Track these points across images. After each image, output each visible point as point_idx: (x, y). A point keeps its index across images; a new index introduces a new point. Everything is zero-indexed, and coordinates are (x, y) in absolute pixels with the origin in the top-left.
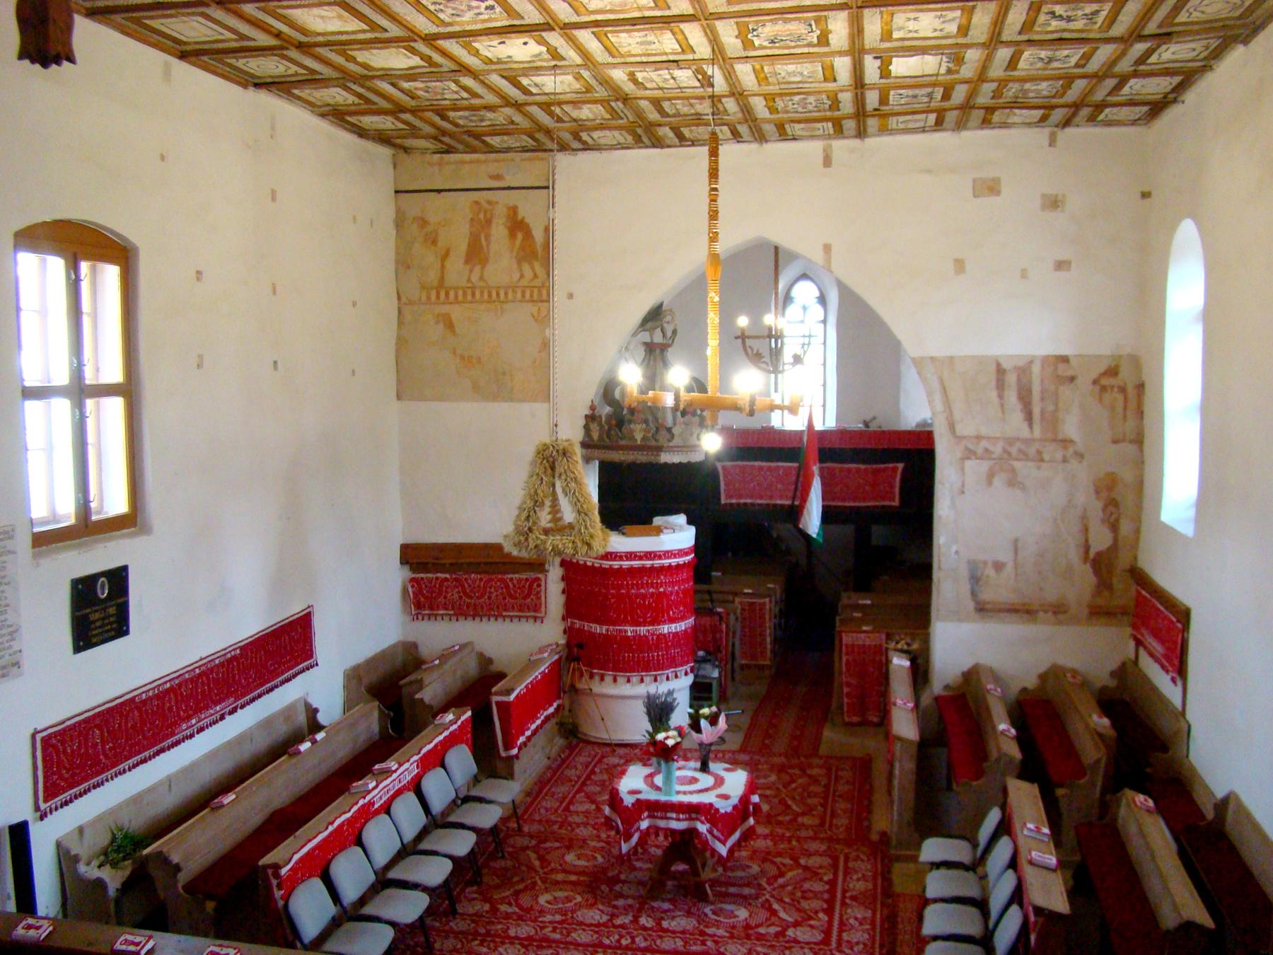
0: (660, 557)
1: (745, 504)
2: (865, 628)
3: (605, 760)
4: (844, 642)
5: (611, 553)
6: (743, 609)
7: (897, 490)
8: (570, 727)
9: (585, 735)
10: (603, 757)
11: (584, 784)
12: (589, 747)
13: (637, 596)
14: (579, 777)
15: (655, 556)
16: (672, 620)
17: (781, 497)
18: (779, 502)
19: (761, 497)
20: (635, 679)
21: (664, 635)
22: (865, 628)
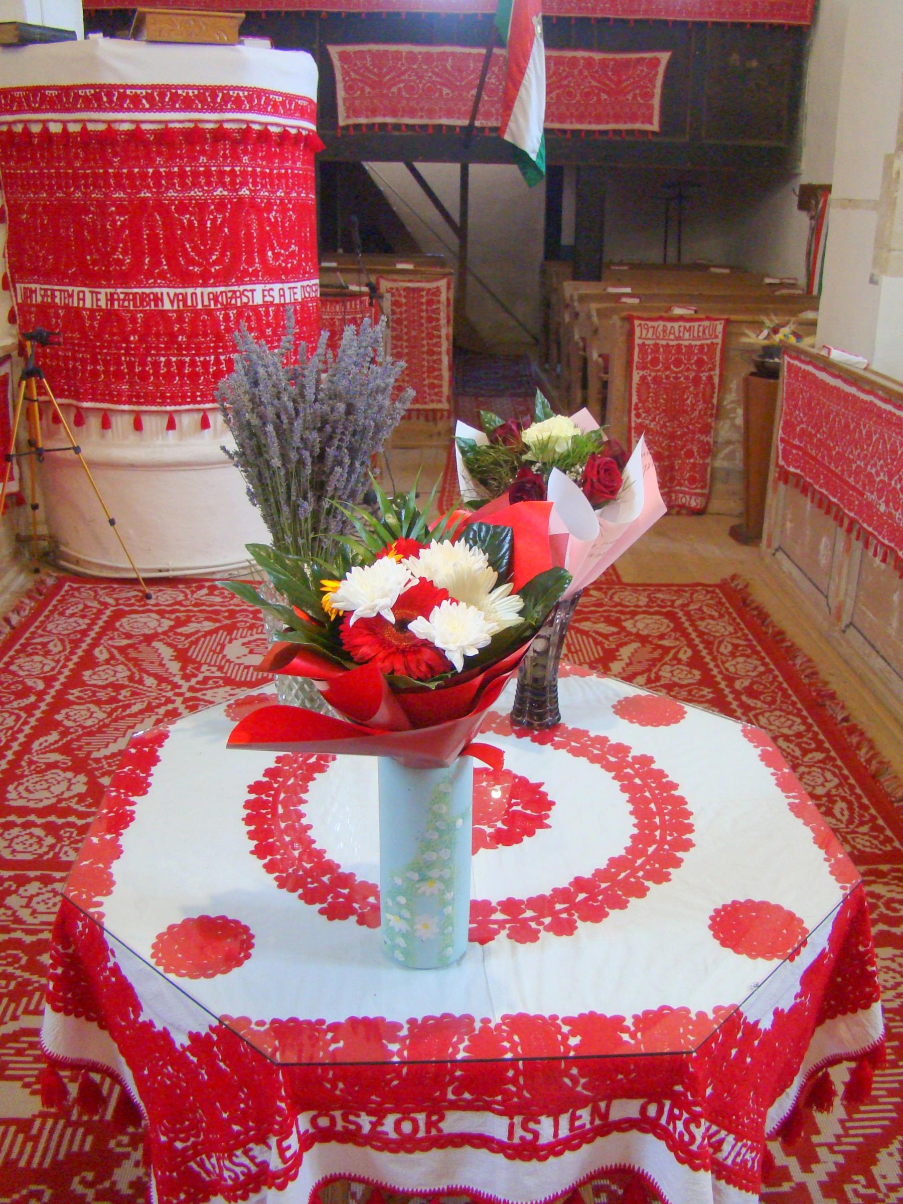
0: (238, 106)
1: (383, 126)
2: (678, 311)
3: (124, 623)
4: (638, 341)
5: (109, 89)
6: (396, 303)
7: (656, 102)
8: (44, 544)
9: (78, 562)
10: (118, 615)
11: (60, 702)
12: (86, 592)
13: (183, 208)
14: (49, 681)
15: (226, 99)
16: (274, 274)
17: (449, 113)
18: (444, 121)
19: (412, 113)
20: (188, 421)
21: (255, 308)
22: (678, 311)
